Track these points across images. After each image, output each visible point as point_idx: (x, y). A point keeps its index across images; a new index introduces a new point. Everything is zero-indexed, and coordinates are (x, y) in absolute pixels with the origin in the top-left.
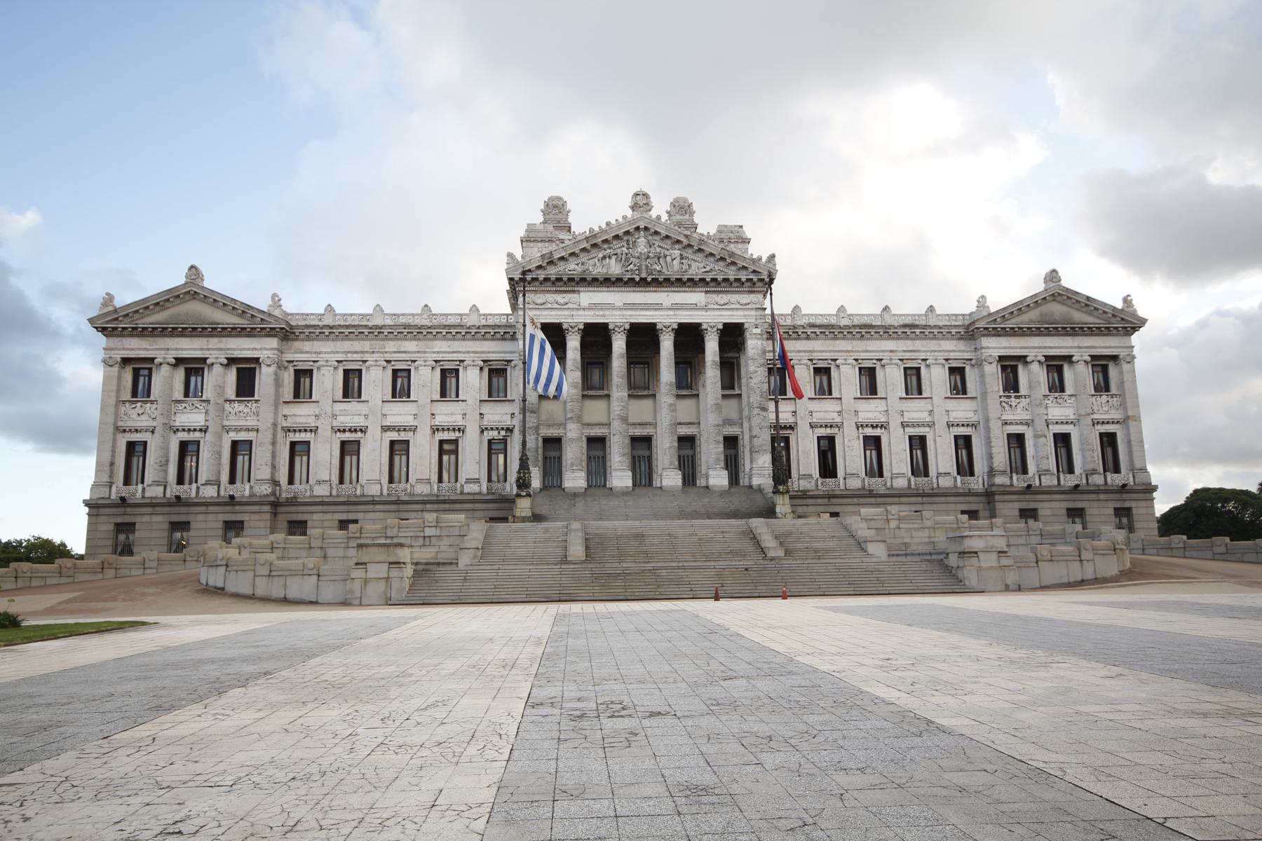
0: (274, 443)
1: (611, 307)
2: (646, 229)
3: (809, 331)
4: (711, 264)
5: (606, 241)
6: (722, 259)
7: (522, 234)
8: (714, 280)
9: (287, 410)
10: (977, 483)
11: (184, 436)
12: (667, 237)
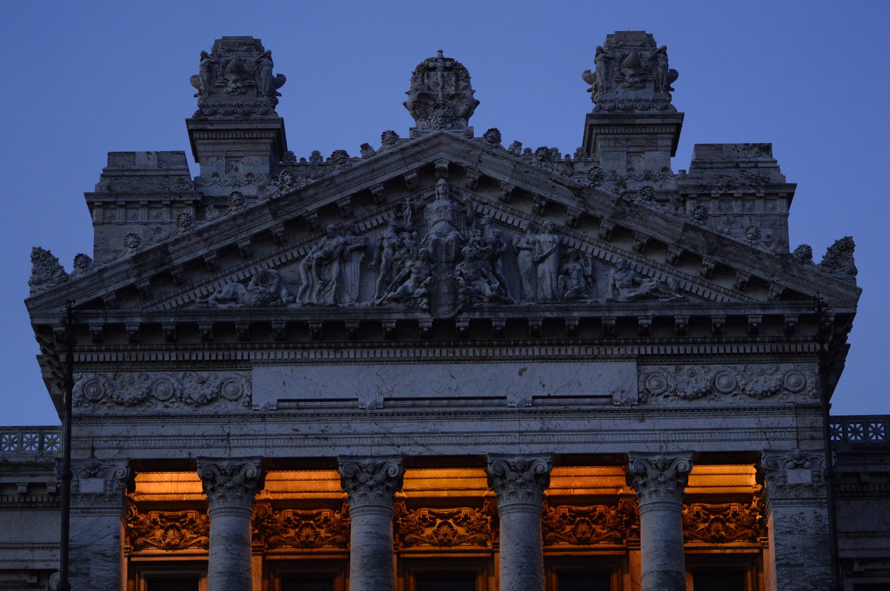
1: (347, 409)
2: (455, 170)
5: (331, 210)
6: (688, 258)
8: (662, 322)
12: (518, 195)
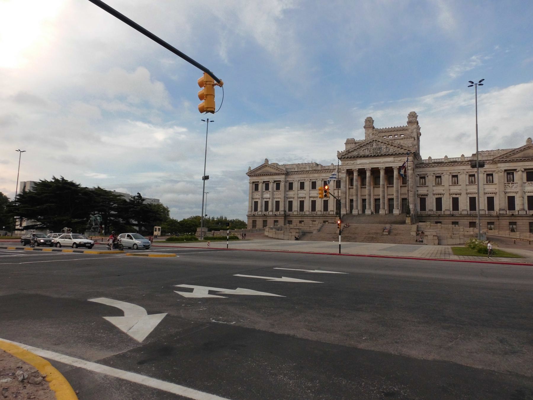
0: (284, 201)
3: (433, 165)
4: (396, 149)
6: (399, 147)
7: (345, 142)
9: (288, 193)
10: (494, 213)
11: (265, 200)
